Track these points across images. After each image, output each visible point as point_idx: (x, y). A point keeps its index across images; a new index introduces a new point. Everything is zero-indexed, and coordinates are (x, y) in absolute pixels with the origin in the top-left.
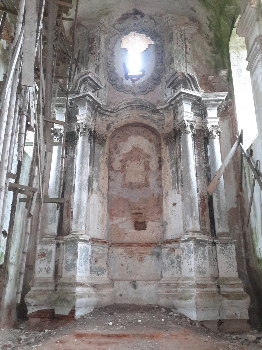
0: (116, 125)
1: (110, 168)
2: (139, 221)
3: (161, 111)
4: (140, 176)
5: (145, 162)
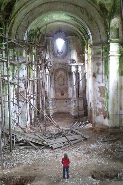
0: (56, 69)
1: (55, 80)
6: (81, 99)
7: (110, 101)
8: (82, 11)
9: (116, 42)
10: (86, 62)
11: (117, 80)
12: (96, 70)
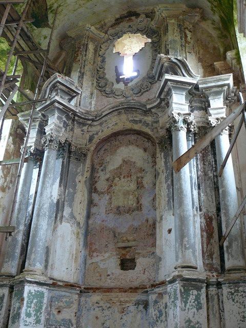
0: (102, 135)
2: (128, 257)
3: (153, 110)
4: (131, 197)
5: (138, 178)
6: (235, 276)
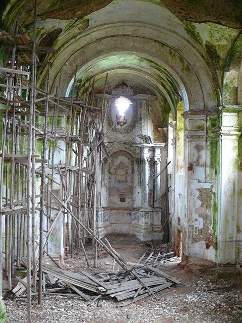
0: (113, 152)
1: (110, 173)
6: (157, 209)
7: (220, 215)
8: (173, 53)
9: (233, 111)
10: (170, 142)
11: (233, 178)
12: (195, 159)
